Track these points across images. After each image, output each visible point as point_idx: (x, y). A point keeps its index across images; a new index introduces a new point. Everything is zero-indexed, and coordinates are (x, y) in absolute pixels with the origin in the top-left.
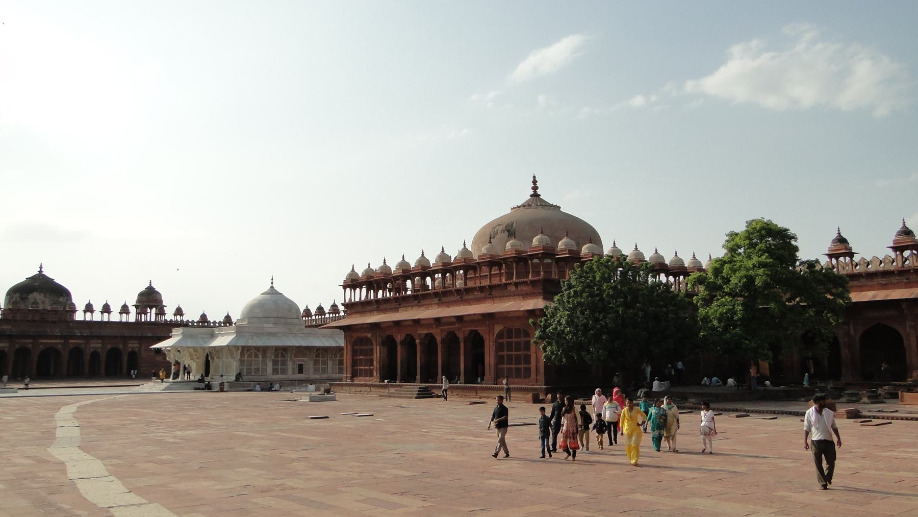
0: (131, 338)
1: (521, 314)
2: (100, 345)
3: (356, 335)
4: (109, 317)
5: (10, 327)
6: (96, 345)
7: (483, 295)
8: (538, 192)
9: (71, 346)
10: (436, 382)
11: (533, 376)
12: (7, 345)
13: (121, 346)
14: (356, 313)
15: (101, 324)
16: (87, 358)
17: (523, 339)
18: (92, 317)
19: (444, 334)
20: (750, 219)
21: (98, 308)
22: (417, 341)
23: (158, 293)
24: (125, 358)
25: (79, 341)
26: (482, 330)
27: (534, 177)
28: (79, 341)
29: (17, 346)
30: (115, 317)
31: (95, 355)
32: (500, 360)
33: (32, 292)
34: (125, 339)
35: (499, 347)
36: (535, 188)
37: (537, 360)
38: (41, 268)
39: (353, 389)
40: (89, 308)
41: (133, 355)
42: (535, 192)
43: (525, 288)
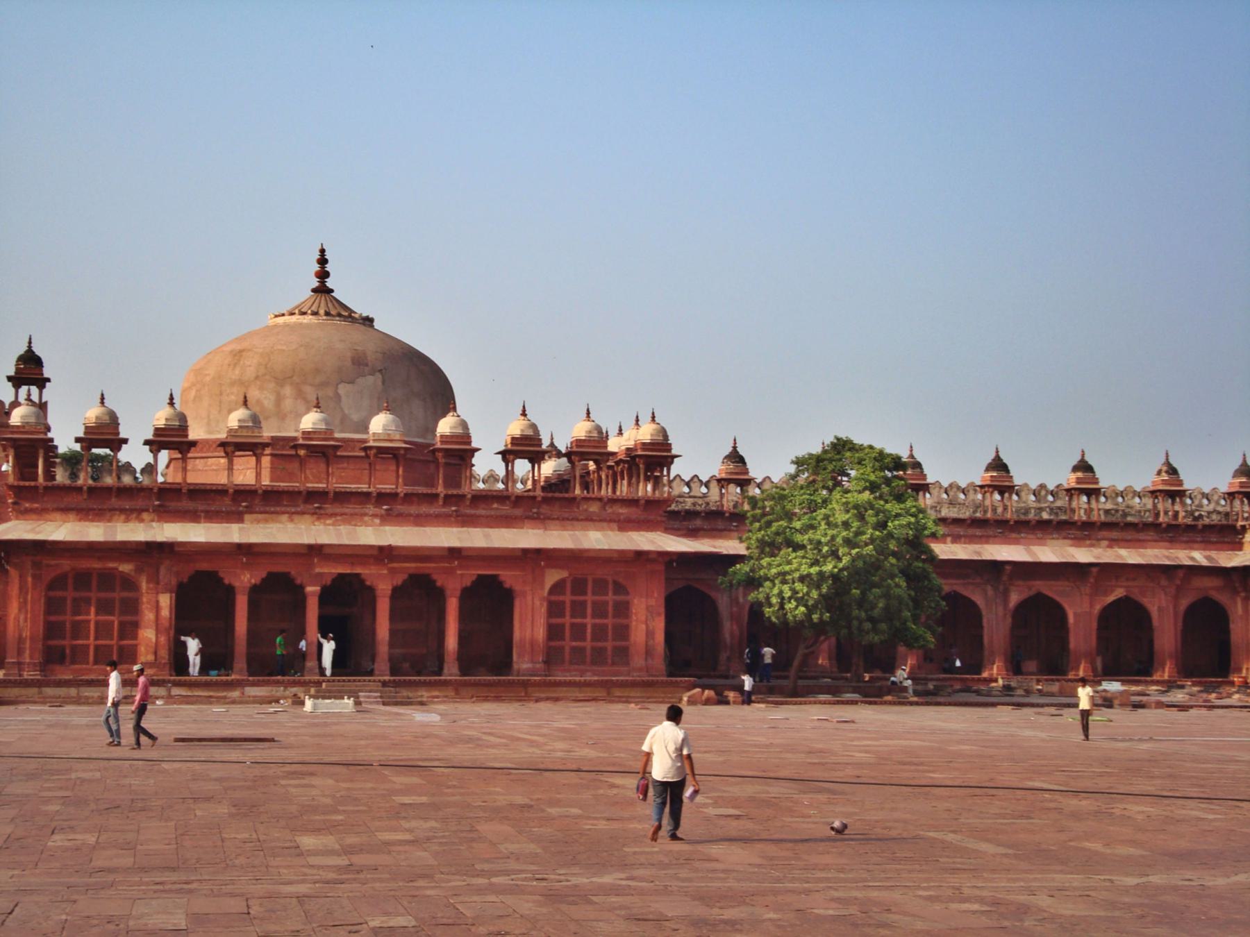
1: (615, 555)
3: (66, 564)
7: (518, 512)
8: (330, 283)
10: (440, 675)
11: (638, 661)
14: (65, 510)
17: (610, 597)
19: (399, 580)
20: (843, 436)
22: (312, 589)
26: (509, 577)
27: (323, 251)
32: (554, 632)
35: (554, 609)
36: (323, 275)
37: (650, 634)
39: (49, 691)
42: (323, 283)
43: (623, 511)
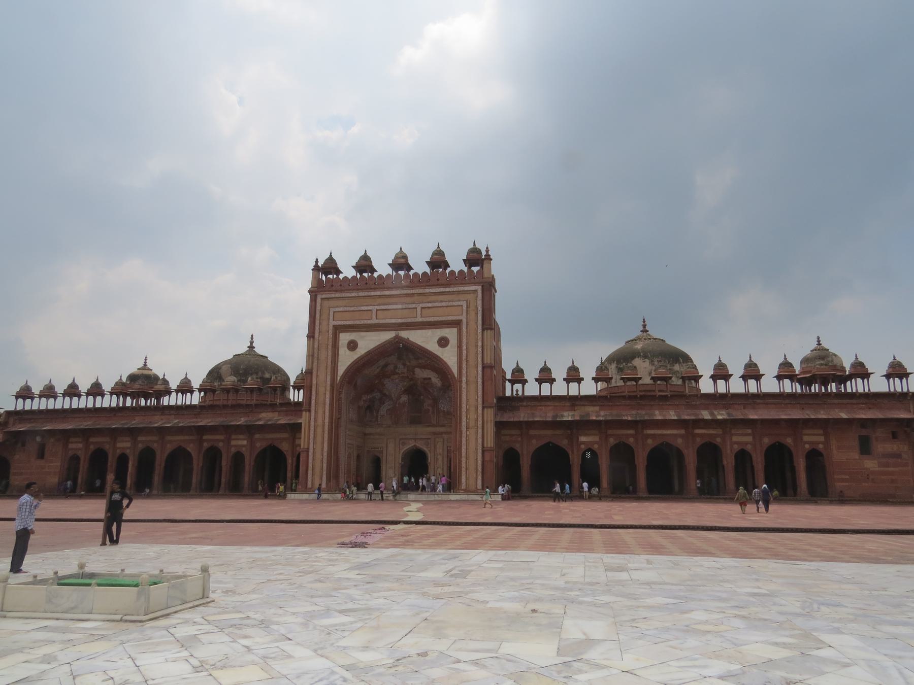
0: (807, 423)
2: (749, 439)
4: (759, 386)
5: (597, 408)
6: (742, 439)
9: (699, 441)
12: (597, 439)
13: (789, 441)
15: (746, 398)
16: (729, 462)
18: (727, 386)
21: (736, 369)
23: (836, 355)
24: (801, 465)
25: (712, 432)
28: (712, 432)
29: (612, 441)
30: (769, 385)
31: (743, 457)
33: (633, 358)
34: (794, 425)
38: (644, 326)
40: (721, 373)
41: (815, 457)
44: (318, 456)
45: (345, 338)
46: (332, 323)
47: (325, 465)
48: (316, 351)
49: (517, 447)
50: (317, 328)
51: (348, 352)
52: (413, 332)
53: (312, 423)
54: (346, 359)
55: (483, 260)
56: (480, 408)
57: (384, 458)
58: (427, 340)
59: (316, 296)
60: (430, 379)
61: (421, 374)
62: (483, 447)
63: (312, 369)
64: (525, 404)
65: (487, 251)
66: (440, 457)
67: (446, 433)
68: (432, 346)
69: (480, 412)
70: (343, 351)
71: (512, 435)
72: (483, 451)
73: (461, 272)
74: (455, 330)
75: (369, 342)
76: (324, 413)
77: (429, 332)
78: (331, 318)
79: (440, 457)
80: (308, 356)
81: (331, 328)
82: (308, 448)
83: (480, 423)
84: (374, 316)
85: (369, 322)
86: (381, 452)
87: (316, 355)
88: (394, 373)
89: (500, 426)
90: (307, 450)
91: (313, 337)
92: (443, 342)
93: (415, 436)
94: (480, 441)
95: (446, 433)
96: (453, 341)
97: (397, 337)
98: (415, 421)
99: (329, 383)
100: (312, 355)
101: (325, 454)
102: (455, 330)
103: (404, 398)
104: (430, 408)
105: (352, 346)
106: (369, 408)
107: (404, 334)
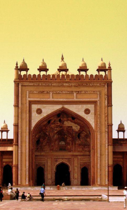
44: (24, 169)
45: (35, 107)
46: (28, 99)
47: (27, 173)
48: (20, 114)
49: (121, 163)
50: (20, 102)
51: (37, 115)
52: (71, 105)
53: (20, 151)
54: (36, 118)
55: (107, 70)
56: (107, 145)
57: (46, 168)
58: (78, 110)
59: (18, 84)
60: (72, 127)
61: (68, 124)
62: (108, 165)
63: (18, 123)
64: (125, 142)
65: (109, 65)
66: (76, 168)
67: (80, 155)
68: (82, 114)
69: (107, 147)
70: (34, 114)
71: (118, 158)
72: (108, 167)
73: (96, 75)
74: (93, 106)
75: (48, 110)
76: (26, 146)
77: (80, 106)
78: (28, 96)
79: (76, 168)
80: (15, 116)
81: (28, 102)
82: (18, 165)
83: (107, 153)
84: (51, 97)
85: (49, 100)
86: (44, 165)
87: (20, 116)
88: (53, 124)
89: (115, 153)
90: (17, 167)
91: (18, 106)
92: (87, 111)
93: (62, 157)
94: (107, 162)
95: (80, 155)
96: (92, 111)
97: (63, 108)
98: (62, 149)
99: (28, 131)
100: (17, 116)
101: (27, 167)
102: (93, 106)
103: (56, 136)
104: (71, 142)
105: (39, 111)
106: (38, 142)
107: (66, 106)
